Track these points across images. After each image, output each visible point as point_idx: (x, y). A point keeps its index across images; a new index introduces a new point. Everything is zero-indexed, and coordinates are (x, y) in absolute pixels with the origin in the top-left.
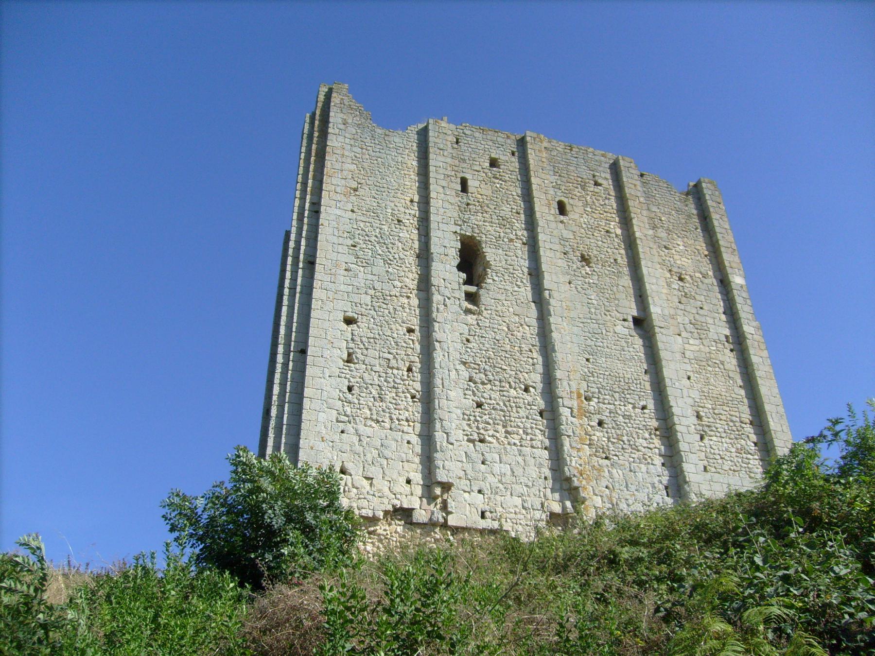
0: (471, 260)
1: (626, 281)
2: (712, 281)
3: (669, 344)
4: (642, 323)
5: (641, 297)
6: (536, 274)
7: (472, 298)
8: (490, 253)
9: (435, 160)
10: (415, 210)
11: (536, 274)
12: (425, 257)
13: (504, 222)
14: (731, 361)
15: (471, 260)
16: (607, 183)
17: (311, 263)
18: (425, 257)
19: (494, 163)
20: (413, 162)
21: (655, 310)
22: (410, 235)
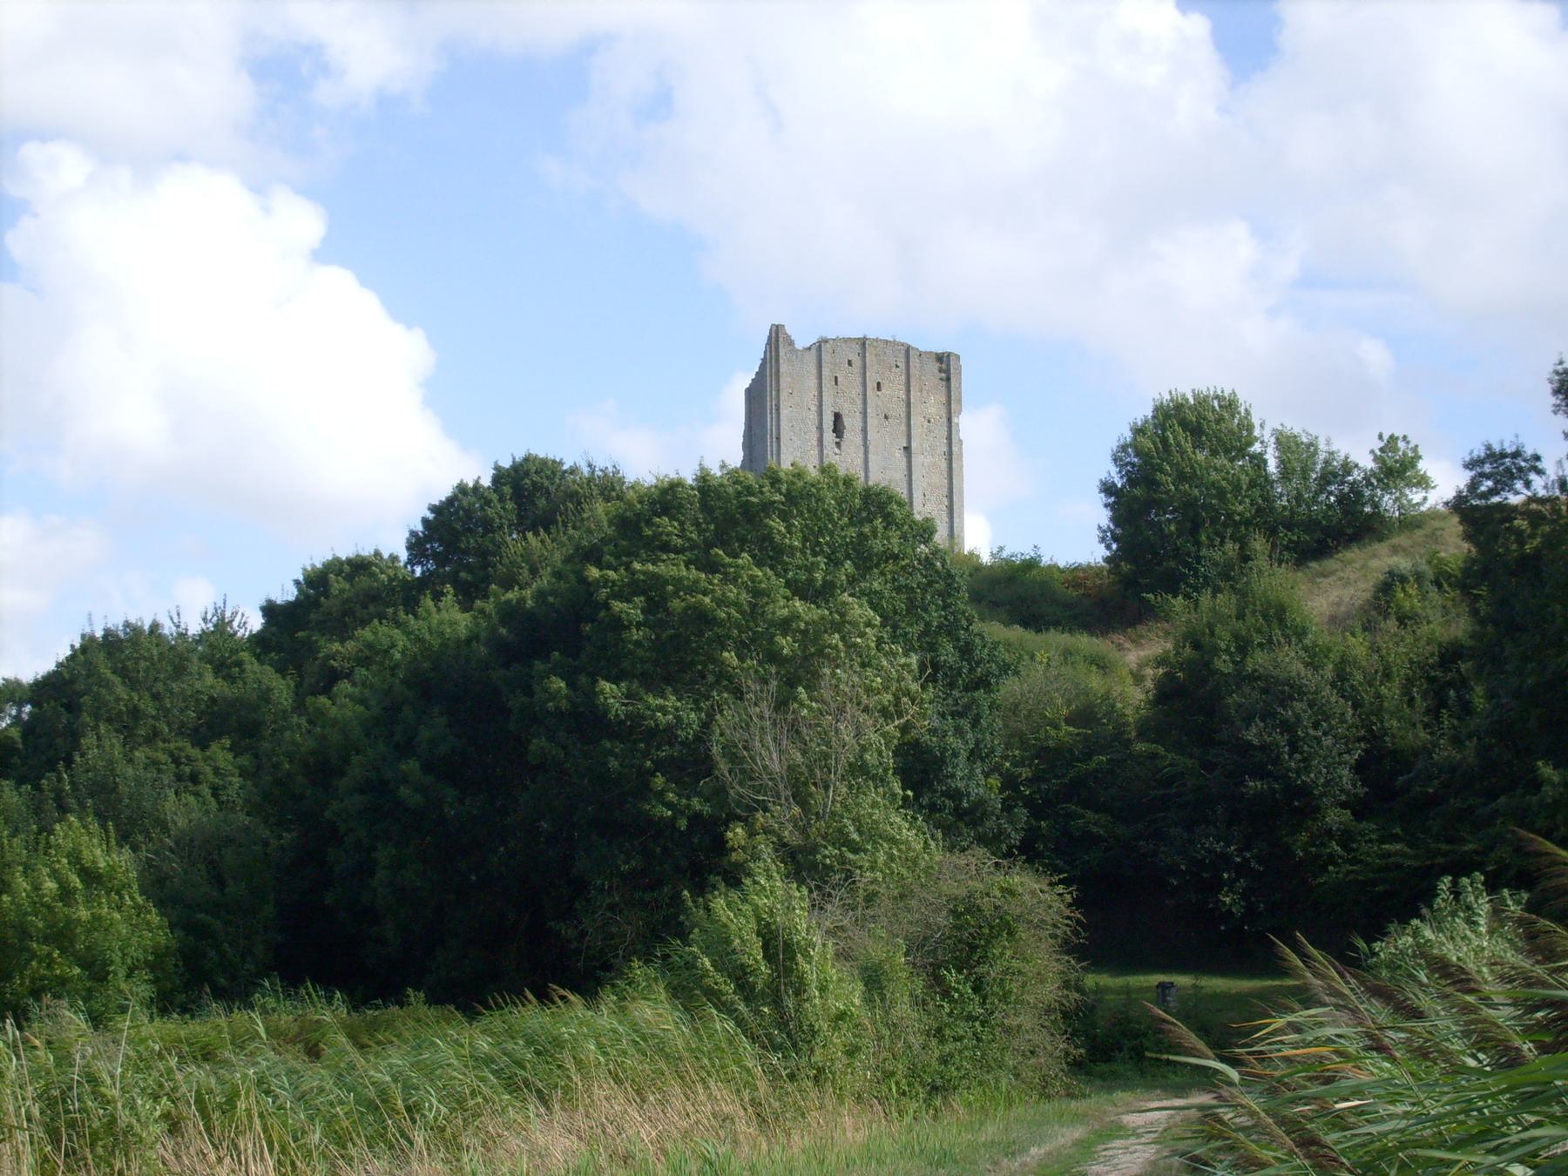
0: (838, 428)
1: (903, 427)
2: (945, 420)
3: (917, 460)
4: (907, 449)
5: (909, 442)
6: (864, 430)
7: (838, 445)
8: (846, 421)
9: (826, 372)
10: (816, 402)
11: (864, 430)
12: (820, 428)
13: (853, 402)
14: (944, 465)
15: (838, 428)
16: (902, 365)
17: (778, 439)
18: (820, 428)
19: (850, 363)
20: (814, 371)
21: (914, 445)
22: (813, 416)
